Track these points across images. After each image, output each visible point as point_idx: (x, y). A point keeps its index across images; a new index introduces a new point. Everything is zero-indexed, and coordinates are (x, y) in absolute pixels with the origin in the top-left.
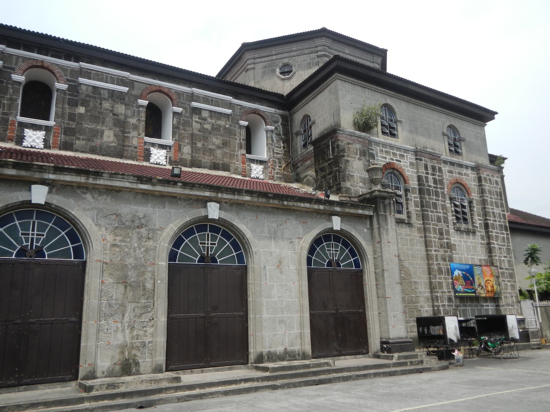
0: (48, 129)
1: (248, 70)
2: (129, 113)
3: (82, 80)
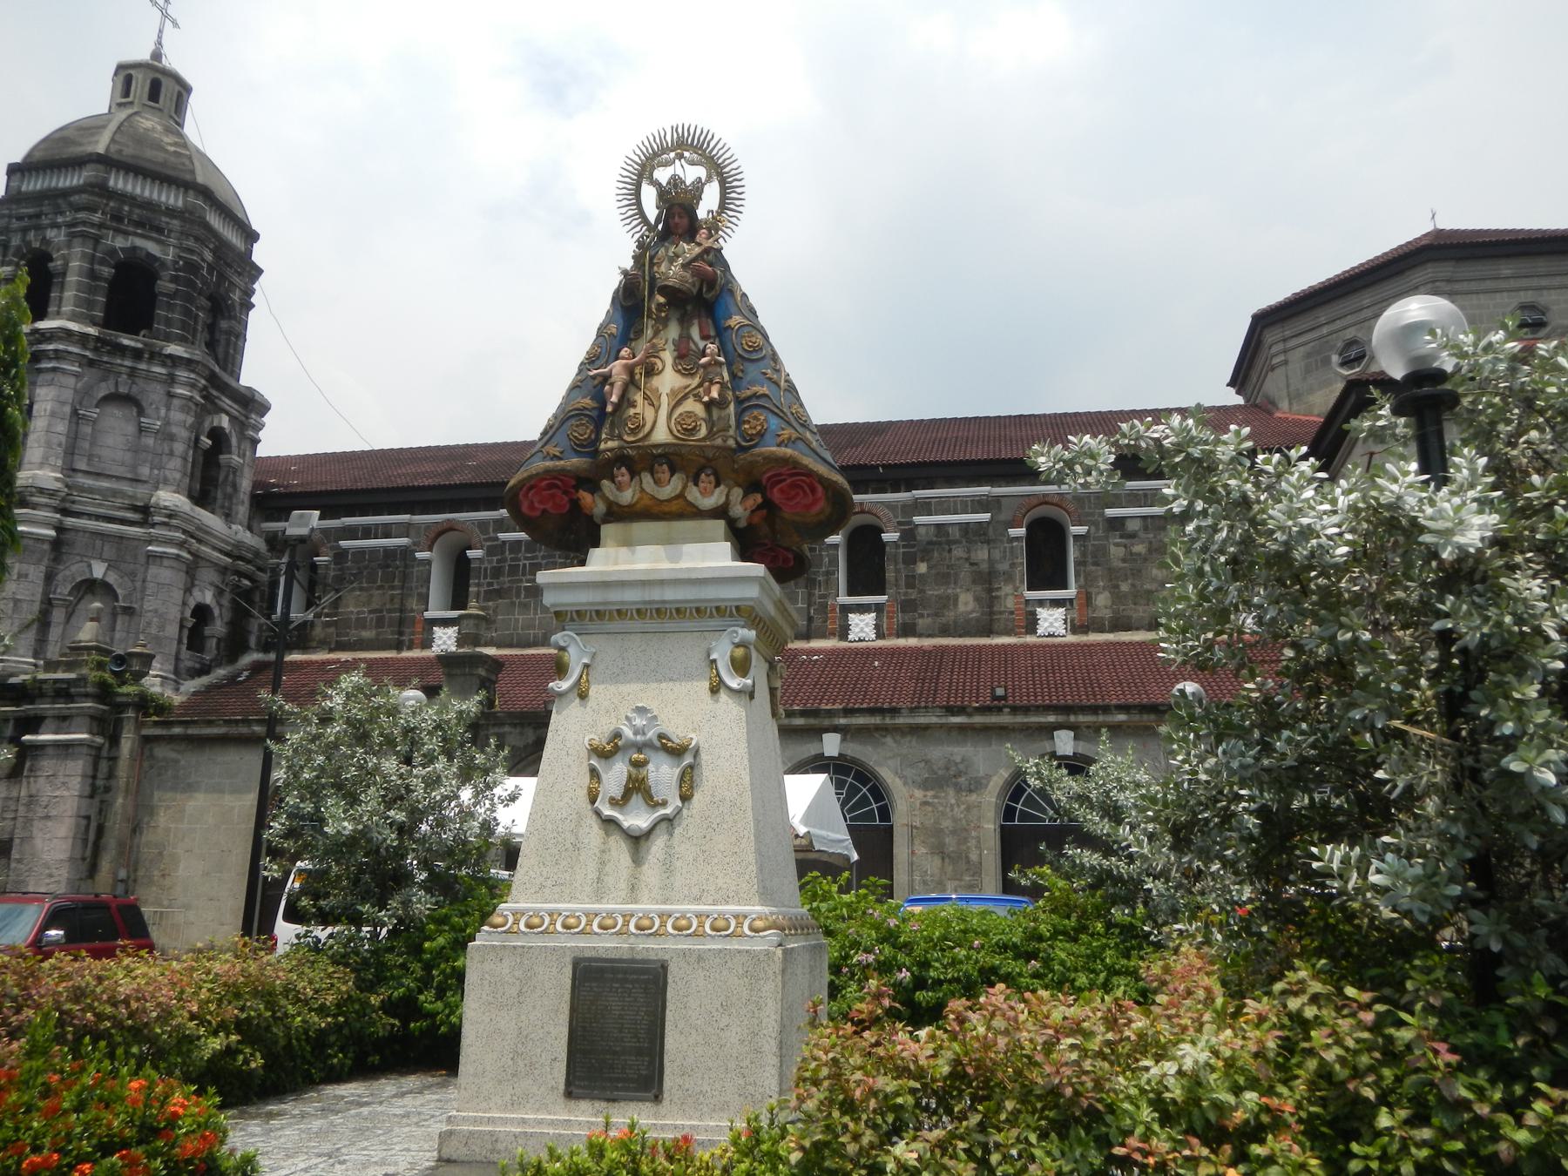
0: (878, 608)
1: (1273, 369)
2: (997, 554)
3: (918, 519)
